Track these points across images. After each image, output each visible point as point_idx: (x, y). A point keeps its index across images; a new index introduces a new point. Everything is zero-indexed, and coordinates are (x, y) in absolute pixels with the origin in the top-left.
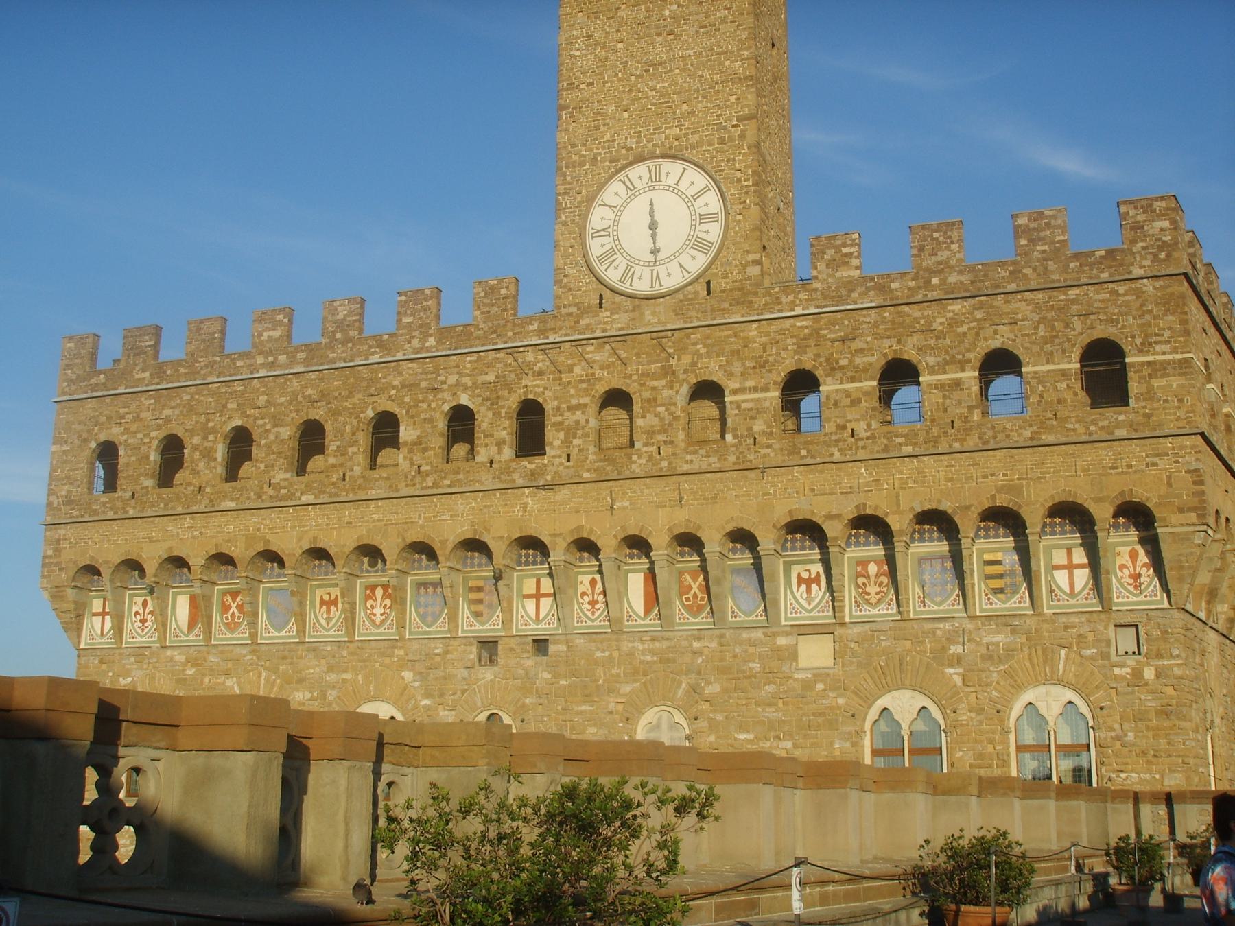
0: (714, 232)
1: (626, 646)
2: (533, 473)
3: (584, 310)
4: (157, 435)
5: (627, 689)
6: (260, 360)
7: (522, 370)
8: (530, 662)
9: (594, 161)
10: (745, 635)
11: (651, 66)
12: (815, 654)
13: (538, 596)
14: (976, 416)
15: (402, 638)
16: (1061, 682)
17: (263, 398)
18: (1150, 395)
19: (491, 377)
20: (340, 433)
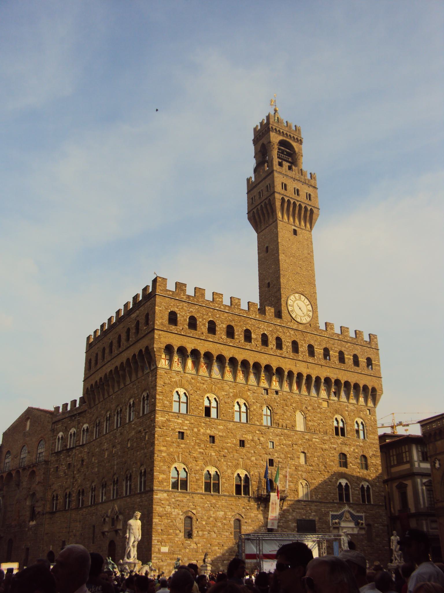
0: (311, 314)
1: (294, 396)
2: (281, 354)
3: (289, 321)
4: (189, 315)
5: (294, 405)
6: (217, 305)
7: (277, 330)
8: (275, 396)
9: (288, 289)
10: (314, 398)
11: (297, 273)
12: (325, 404)
13: (276, 381)
14: (353, 365)
15: (247, 384)
16: (361, 418)
17: (218, 316)
18: (375, 369)
19: (271, 329)
20: (238, 331)
